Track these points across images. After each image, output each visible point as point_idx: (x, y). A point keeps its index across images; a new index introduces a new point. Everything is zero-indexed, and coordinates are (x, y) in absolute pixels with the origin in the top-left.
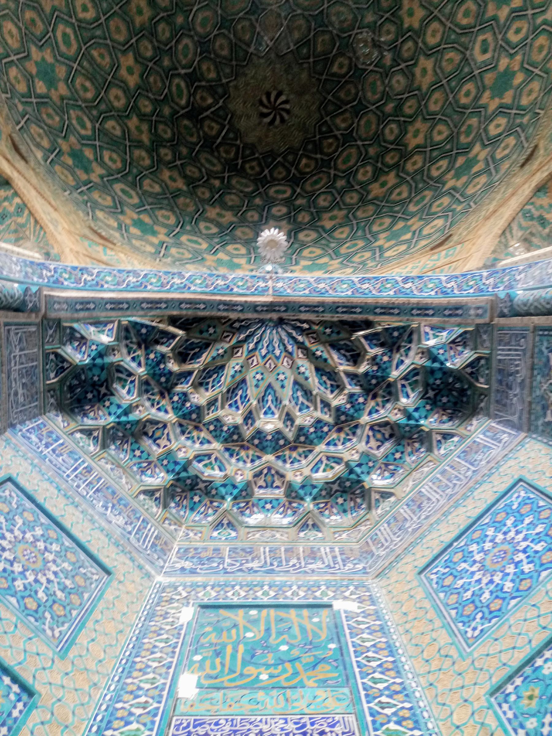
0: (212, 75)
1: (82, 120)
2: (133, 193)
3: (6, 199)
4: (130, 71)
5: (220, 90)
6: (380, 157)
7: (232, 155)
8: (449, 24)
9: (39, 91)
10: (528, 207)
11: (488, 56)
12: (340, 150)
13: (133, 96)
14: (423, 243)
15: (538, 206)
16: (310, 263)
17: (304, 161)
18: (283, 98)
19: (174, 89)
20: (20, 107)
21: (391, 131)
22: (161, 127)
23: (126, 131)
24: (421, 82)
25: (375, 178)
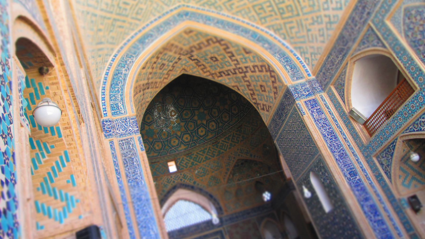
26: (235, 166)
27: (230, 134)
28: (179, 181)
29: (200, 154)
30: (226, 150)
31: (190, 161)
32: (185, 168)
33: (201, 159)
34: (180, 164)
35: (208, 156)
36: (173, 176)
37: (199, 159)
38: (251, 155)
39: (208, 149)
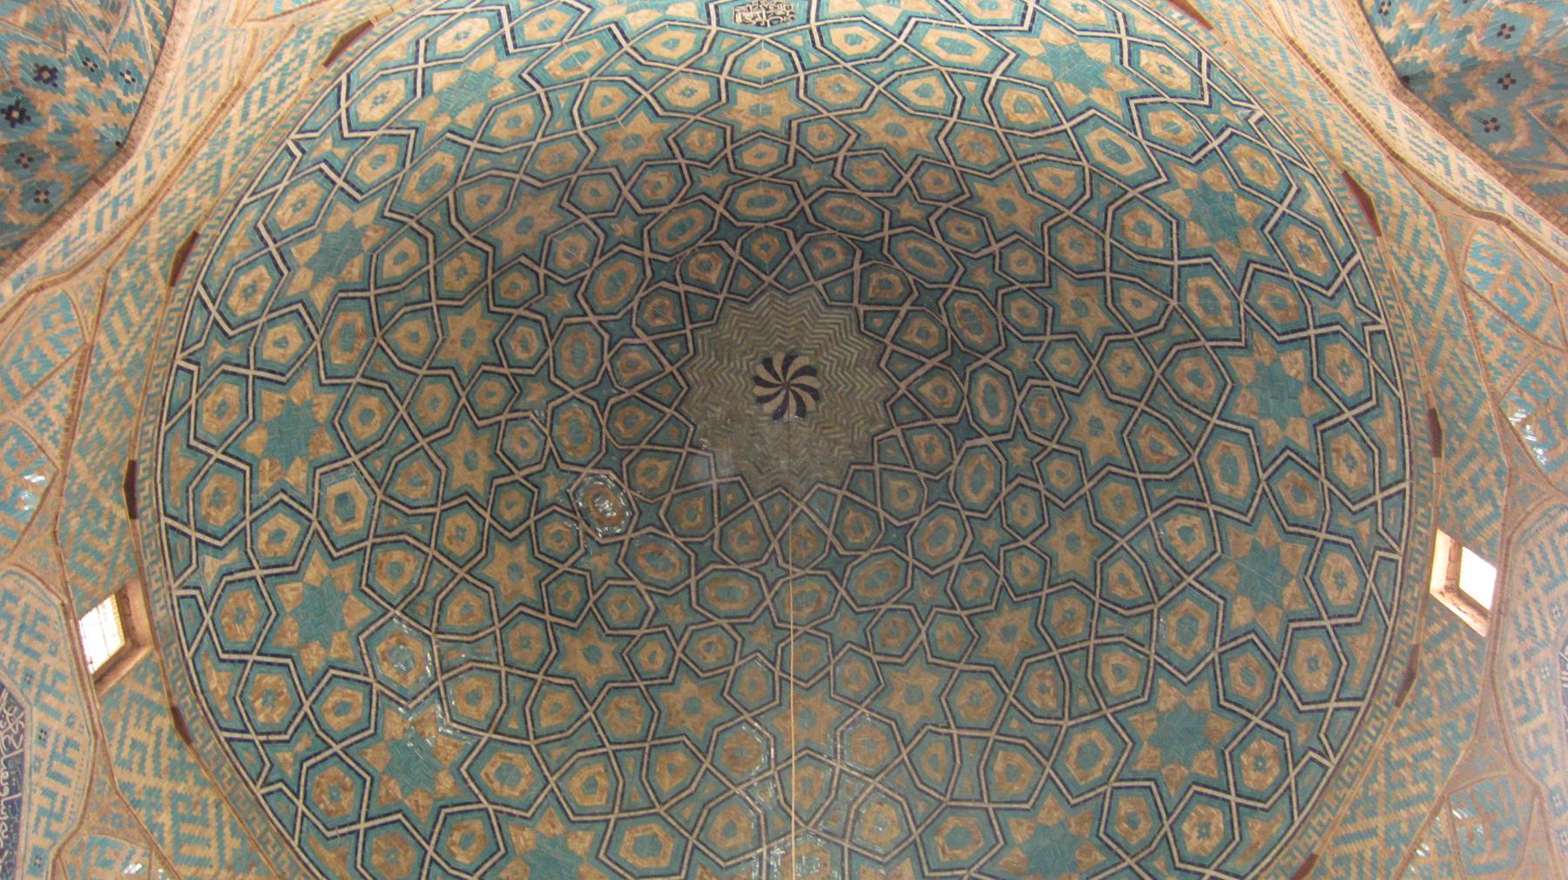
0: (920, 439)
1: (1206, 310)
2: (1100, 156)
3: (1414, 39)
4: (1096, 426)
5: (904, 411)
6: (543, 289)
7: (875, 277)
8: (431, 552)
9: (1299, 355)
10: (134, 98)
11: (335, 489)
12: (635, 304)
13: (1096, 376)
14: (395, 52)
15: (112, 105)
16: (672, 11)
17: (713, 277)
18: (769, 408)
19: (1003, 404)
20: (1345, 308)
21: (525, 343)
22: (1033, 323)
23: (1111, 303)
24: (475, 442)
25: (546, 242)
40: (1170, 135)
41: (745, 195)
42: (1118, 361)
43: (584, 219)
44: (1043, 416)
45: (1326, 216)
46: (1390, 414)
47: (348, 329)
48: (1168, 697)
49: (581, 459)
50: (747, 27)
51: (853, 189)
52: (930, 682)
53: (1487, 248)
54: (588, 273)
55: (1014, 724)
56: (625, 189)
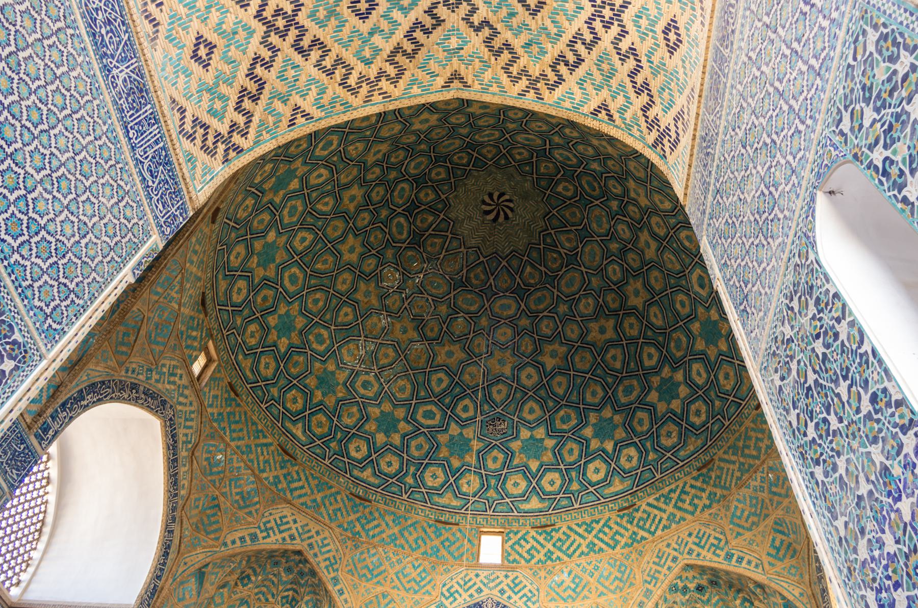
0: (432, 196)
1: (320, 335)
3: (300, 561)
4: (352, 250)
5: (440, 206)
12: (564, 270)
17: (528, 269)
19: (394, 229)
26: (673, 588)
27: (673, 486)
28: (496, 592)
29: (576, 533)
30: (653, 533)
31: (543, 546)
32: (523, 561)
33: (575, 546)
34: (512, 547)
35: (596, 541)
36: (483, 574)
37: (572, 544)
38: (729, 557)
39: (601, 524)
40: (351, 411)
41: (511, 312)
42: (348, 282)
43: (579, 319)
44: (376, 237)
45: (294, 431)
46: (248, 373)
47: (678, 348)
48: (295, 184)
49: (599, 210)
50: (503, 418)
51: (466, 316)
52: (417, 126)
53: (254, 497)
54: (581, 293)
55: (368, 133)
56: (560, 329)
